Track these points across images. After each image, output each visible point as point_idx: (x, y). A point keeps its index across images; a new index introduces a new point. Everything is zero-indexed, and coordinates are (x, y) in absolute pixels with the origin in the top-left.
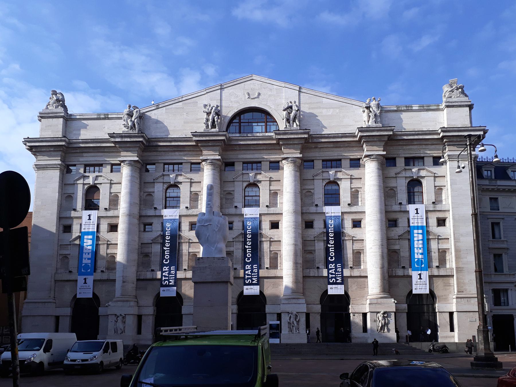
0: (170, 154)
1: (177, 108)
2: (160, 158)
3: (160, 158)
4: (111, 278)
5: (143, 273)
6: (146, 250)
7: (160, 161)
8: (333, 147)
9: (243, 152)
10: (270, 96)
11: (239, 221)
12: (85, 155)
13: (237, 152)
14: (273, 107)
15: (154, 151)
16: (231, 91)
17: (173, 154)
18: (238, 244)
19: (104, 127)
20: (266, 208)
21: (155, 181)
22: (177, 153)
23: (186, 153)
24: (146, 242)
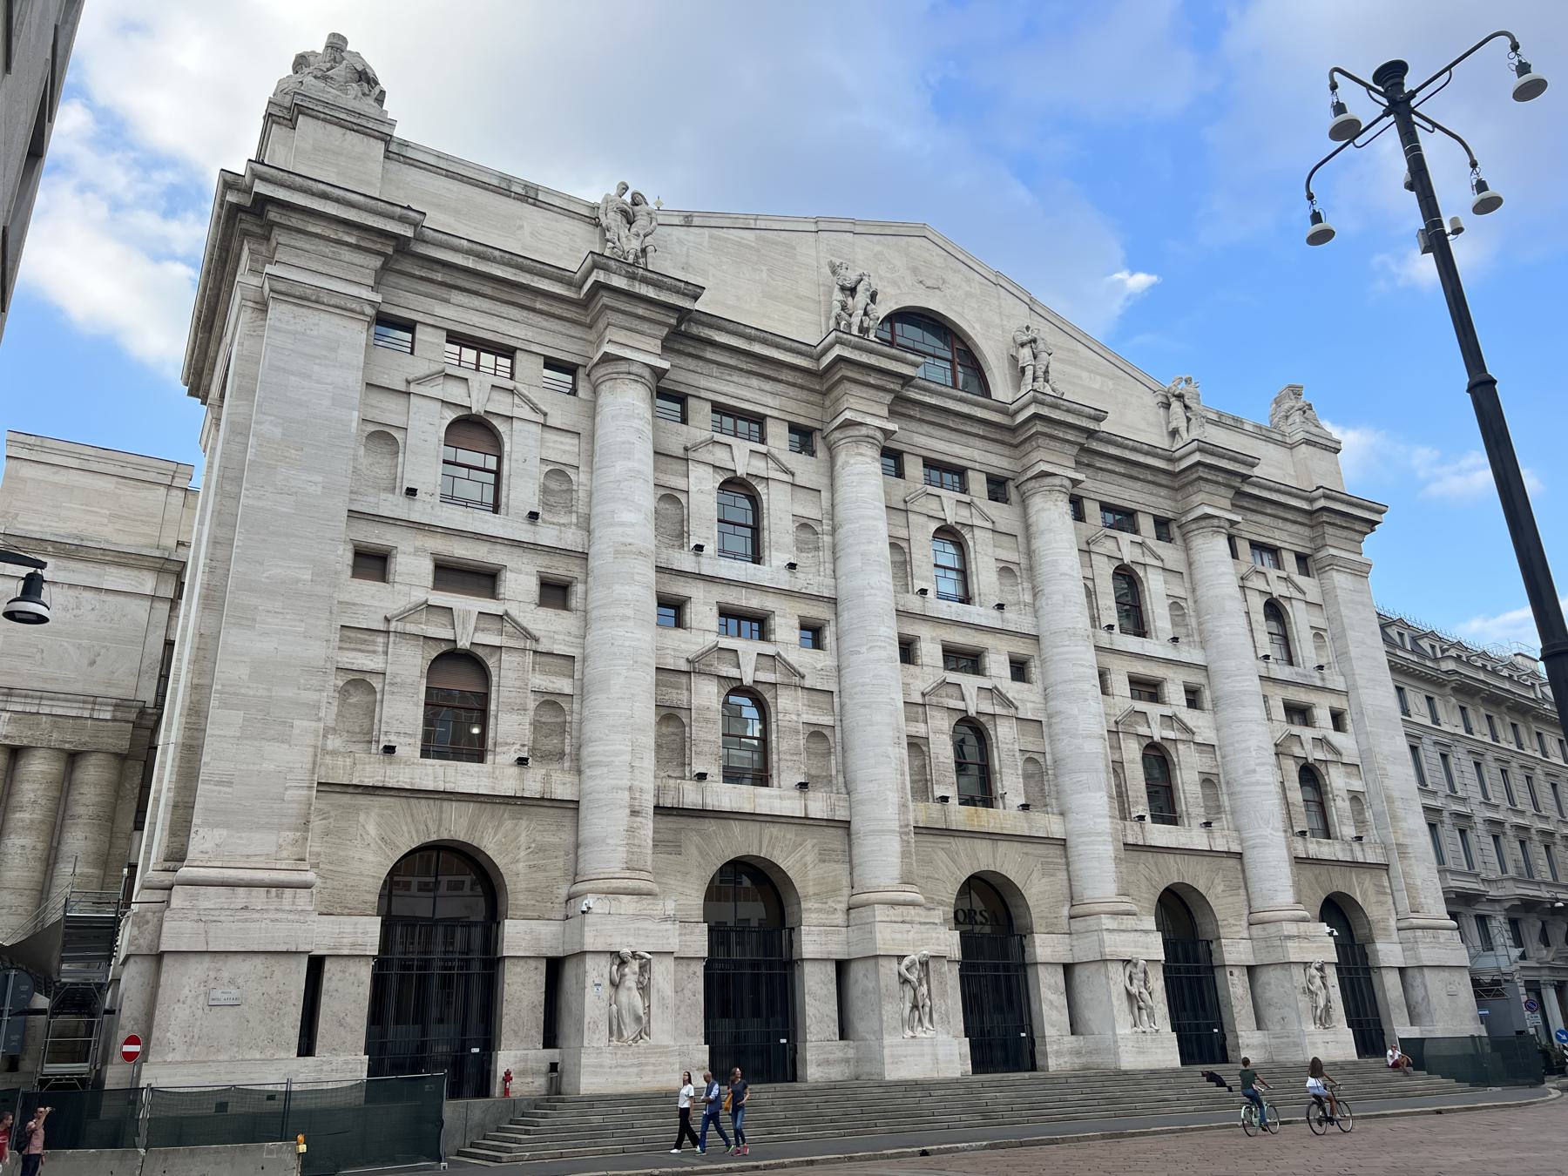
0: (735, 379)
1: (740, 244)
2: (703, 382)
3: (703, 382)
4: (562, 791)
5: (672, 782)
6: (677, 697)
7: (703, 394)
8: (1124, 475)
9: (926, 428)
10: (969, 295)
11: (933, 639)
12: (457, 297)
13: (913, 426)
14: (977, 326)
15: (690, 355)
16: (878, 248)
17: (743, 381)
18: (937, 714)
19: (521, 227)
20: (996, 613)
21: (691, 455)
22: (755, 382)
23: (780, 387)
24: (670, 664)
